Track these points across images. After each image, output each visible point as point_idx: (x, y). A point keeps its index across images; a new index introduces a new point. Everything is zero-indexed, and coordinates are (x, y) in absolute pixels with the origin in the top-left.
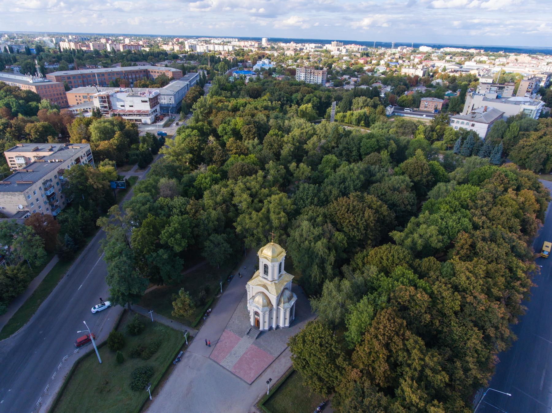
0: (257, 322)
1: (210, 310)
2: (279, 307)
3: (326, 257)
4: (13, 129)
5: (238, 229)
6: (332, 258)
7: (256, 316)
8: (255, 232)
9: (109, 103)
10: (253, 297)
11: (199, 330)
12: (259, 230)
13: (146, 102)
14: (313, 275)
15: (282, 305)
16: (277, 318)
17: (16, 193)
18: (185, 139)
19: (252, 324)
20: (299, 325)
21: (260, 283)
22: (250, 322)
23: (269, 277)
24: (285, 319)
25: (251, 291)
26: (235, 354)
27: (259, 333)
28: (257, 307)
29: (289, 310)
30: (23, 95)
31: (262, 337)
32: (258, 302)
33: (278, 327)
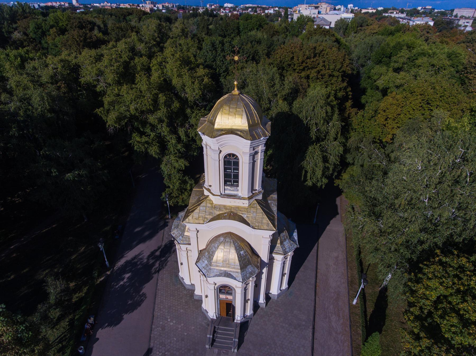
0: (229, 308)
1: (91, 320)
2: (274, 255)
5: (111, 120)
6: (335, 124)
7: (222, 296)
8: (152, 119)
10: (205, 254)
12: (159, 114)
20: (299, 275)
21: (218, 213)
22: (204, 314)
23: (243, 189)
24: (283, 275)
25: (193, 241)
27: (238, 329)
28: (228, 275)
29: (290, 254)
32: (226, 262)
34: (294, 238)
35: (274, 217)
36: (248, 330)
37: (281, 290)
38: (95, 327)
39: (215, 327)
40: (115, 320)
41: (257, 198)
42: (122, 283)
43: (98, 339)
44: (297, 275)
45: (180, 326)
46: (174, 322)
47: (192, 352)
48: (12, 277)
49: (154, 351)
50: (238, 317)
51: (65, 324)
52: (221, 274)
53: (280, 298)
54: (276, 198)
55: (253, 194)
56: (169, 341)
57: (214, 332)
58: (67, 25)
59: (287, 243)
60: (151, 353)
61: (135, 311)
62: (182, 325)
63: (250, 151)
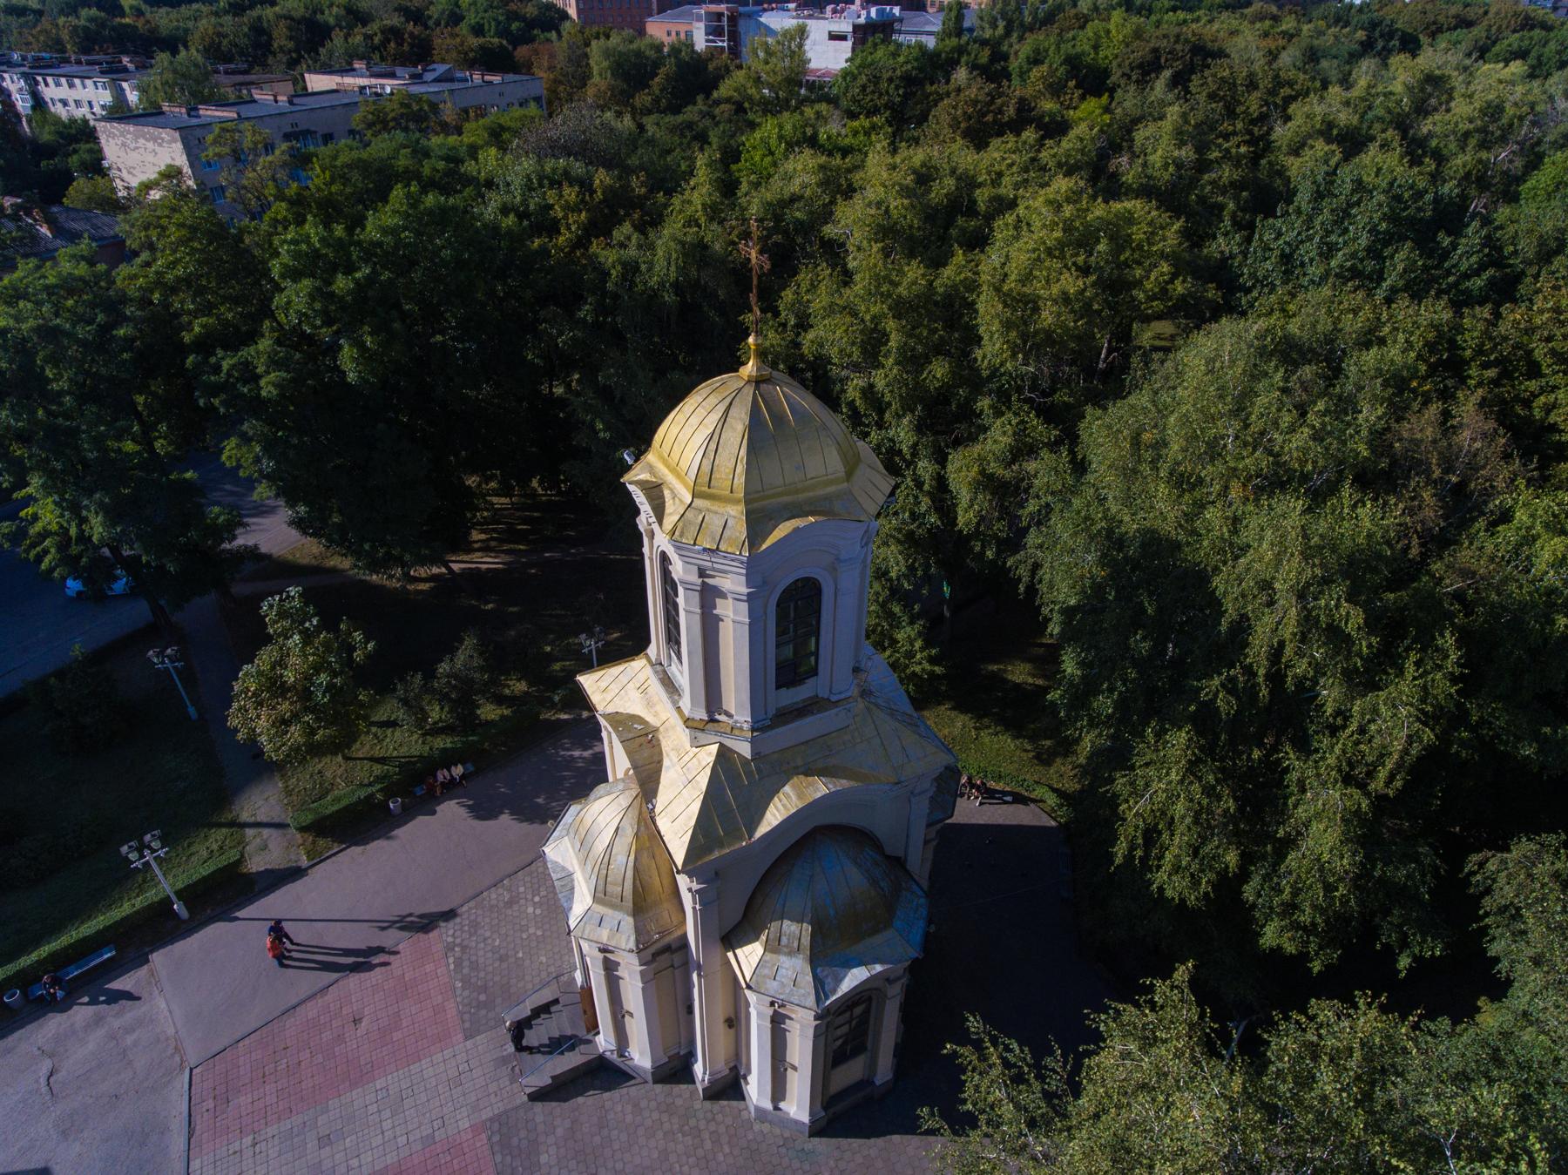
1: (458, 771)
3: (1330, 694)
4: (406, 47)
9: (734, 37)
11: (317, 858)
13: (842, 38)
14: (1135, 812)
15: (749, 957)
16: (736, 1022)
17: (166, 134)
18: (855, 78)
19: (578, 977)
26: (325, 1141)
30: (530, 10)
31: (588, 1103)
33: (729, 1087)
34: (839, 981)
35: (733, 834)
36: (607, 1095)
37: (776, 1108)
38: (451, 788)
39: (556, 1001)
40: (484, 811)
41: (729, 743)
42: (577, 753)
43: (434, 813)
44: (896, 1138)
45: (532, 930)
46: (538, 912)
47: (483, 997)
48: (490, 606)
49: (450, 925)
50: (604, 1041)
51: (443, 742)
52: (563, 868)
53: (766, 1127)
54: (819, 795)
55: (712, 720)
56: (488, 934)
57: (544, 1009)
58: (1116, 57)
59: (795, 970)
60: (447, 920)
61: (525, 825)
62: (539, 933)
63: (685, 571)
